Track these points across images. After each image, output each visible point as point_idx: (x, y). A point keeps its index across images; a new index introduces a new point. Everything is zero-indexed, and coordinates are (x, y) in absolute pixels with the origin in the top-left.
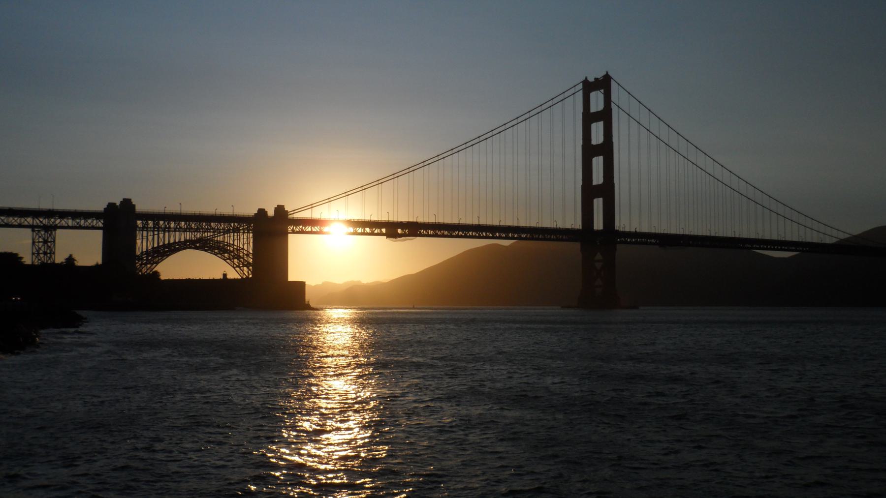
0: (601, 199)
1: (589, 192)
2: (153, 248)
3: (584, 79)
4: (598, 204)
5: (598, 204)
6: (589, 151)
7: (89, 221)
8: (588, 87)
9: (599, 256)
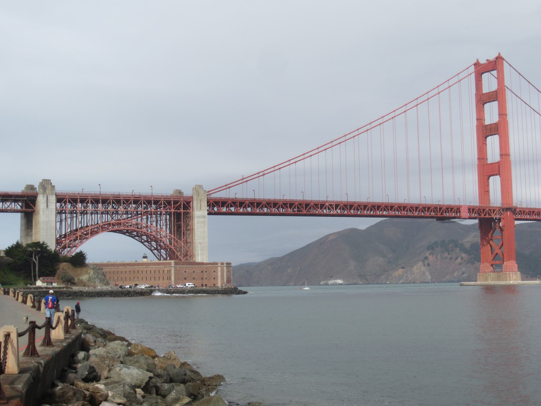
2: (71, 231)
3: (475, 61)
4: (495, 182)
7: (8, 204)
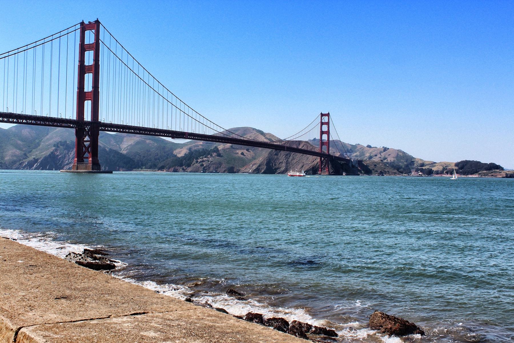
0: (90, 102)
1: (82, 96)
4: (88, 105)
5: (88, 105)
6: (83, 70)
8: (84, 27)
9: (87, 138)
